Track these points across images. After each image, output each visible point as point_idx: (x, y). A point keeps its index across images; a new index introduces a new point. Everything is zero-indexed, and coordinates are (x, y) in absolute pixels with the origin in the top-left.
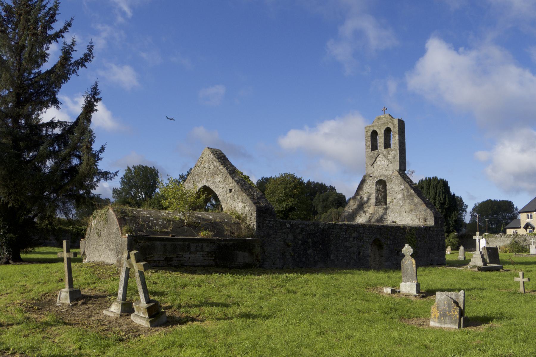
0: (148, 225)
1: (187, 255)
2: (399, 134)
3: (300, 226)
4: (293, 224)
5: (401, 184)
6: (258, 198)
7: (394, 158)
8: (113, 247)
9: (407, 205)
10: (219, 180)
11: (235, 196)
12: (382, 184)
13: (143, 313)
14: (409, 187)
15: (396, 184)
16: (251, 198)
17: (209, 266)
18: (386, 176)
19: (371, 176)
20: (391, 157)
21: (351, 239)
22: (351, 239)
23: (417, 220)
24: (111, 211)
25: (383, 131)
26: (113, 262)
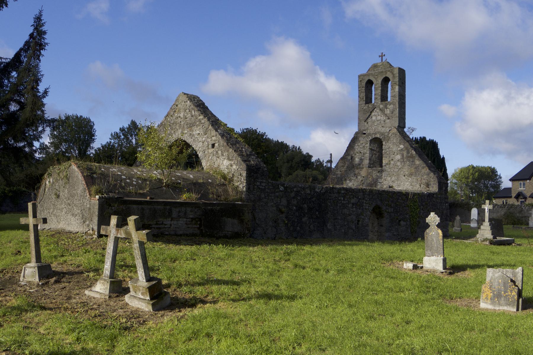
0: (121, 185)
1: (168, 222)
2: (399, 85)
3: (295, 190)
4: (287, 187)
5: (400, 144)
6: (247, 155)
7: (392, 113)
8: (77, 211)
9: (406, 167)
10: (198, 132)
11: (220, 152)
12: (377, 143)
13: (142, 294)
14: (409, 147)
15: (393, 143)
16: (239, 155)
17: (194, 235)
18: (382, 134)
19: (365, 134)
20: (388, 112)
21: (350, 205)
22: (350, 205)
23: (418, 186)
24: (74, 167)
25: (380, 80)
26: (77, 230)
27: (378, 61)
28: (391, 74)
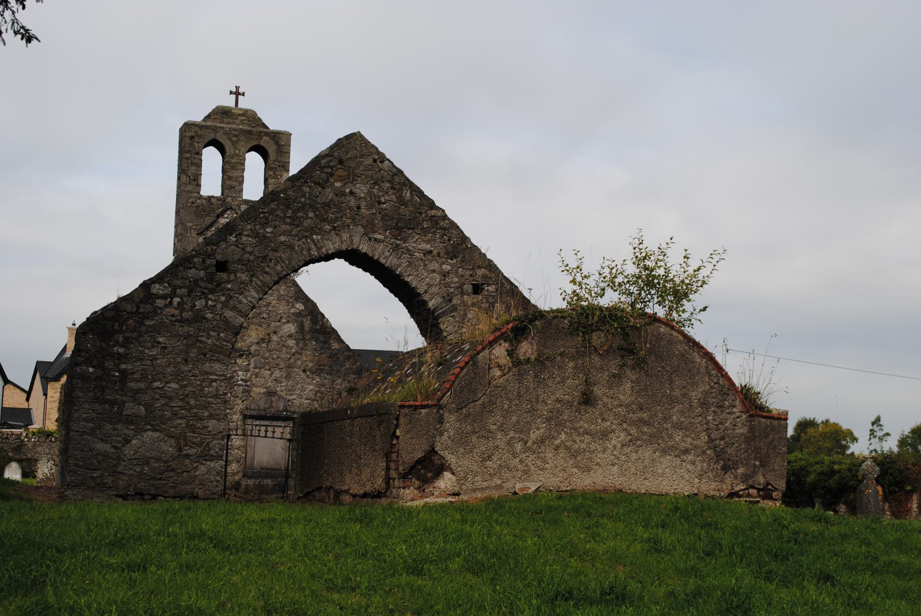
27: (229, 102)
28: (272, 142)
